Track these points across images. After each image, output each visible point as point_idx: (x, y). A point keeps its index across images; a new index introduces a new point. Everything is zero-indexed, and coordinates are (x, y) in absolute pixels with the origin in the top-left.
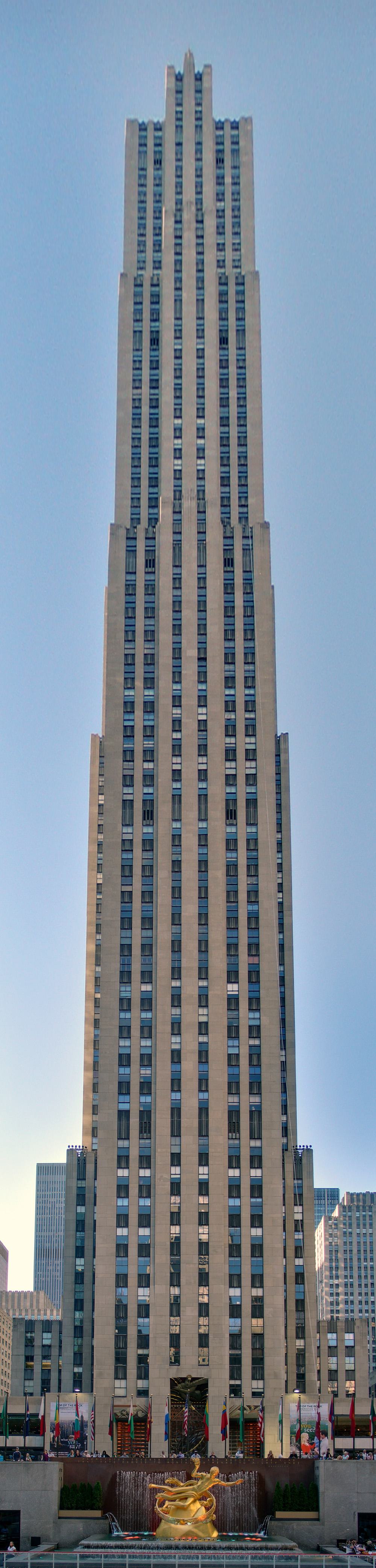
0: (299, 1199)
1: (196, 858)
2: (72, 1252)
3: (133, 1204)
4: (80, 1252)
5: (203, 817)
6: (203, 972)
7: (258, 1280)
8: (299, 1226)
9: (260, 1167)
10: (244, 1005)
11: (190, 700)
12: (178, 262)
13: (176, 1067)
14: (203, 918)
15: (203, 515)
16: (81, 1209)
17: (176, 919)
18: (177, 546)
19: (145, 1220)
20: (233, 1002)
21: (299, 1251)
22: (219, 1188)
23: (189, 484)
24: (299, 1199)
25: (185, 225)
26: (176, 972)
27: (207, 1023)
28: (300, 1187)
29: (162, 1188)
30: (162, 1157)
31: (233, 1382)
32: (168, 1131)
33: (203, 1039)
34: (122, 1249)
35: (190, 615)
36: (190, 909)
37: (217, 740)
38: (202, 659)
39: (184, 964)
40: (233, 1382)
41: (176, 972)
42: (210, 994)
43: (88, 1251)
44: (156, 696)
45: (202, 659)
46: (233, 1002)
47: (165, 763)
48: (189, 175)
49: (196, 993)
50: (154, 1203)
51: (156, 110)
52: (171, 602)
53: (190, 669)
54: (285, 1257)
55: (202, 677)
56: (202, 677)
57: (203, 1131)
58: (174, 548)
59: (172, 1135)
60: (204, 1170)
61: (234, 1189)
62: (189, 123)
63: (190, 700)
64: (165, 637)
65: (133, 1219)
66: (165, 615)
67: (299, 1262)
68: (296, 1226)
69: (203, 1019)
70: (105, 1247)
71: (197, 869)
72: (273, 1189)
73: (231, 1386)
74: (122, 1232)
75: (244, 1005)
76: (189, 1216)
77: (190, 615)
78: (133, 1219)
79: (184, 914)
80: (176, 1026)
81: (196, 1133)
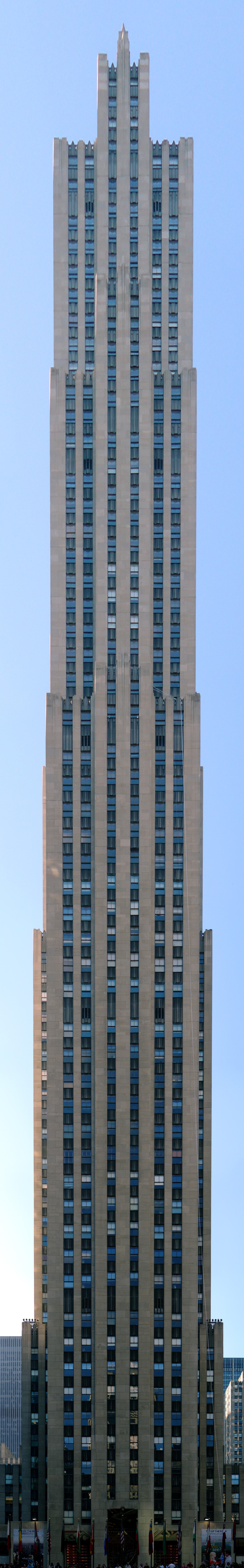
0: (211, 1365)
1: (128, 1056)
2: (28, 1408)
3: (77, 1368)
4: (34, 1408)
5: (134, 1016)
6: (134, 1165)
7: (177, 1431)
8: (210, 1387)
9: (180, 1337)
10: (168, 1195)
11: (123, 894)
12: (112, 355)
13: (111, 1251)
14: (134, 1113)
15: (136, 684)
16: (35, 1373)
17: (111, 1115)
18: (111, 720)
19: (87, 1381)
20: (159, 1192)
21: (210, 1408)
22: (147, 1355)
23: (123, 647)
24: (211, 1365)
25: (119, 302)
26: (111, 1165)
27: (137, 1212)
28: (212, 1355)
29: (101, 1355)
30: (100, 1329)
31: (157, 1513)
33: (134, 1226)
34: (68, 1405)
35: (123, 800)
36: (123, 1106)
37: (148, 937)
38: (135, 850)
39: (118, 1157)
40: (157, 1513)
41: (111, 1165)
42: (140, 1185)
43: (41, 1408)
44: (92, 889)
45: (135, 850)
46: (159, 1192)
47: (101, 961)
49: (128, 1184)
50: (94, 1367)
51: (86, 129)
52: (106, 785)
53: (123, 860)
54: (199, 1412)
55: (135, 869)
56: (135, 869)
57: (134, 1306)
58: (108, 723)
59: (109, 1310)
60: (134, 1340)
61: (159, 1355)
62: (123, 147)
63: (123, 894)
64: (100, 825)
65: (78, 1381)
66: (100, 799)
67: (210, 1416)
68: (208, 1387)
69: (134, 1208)
70: (54, 1404)
71: (129, 1067)
72: (191, 1356)
73: (155, 1515)
74: (69, 1391)
75: (168, 1195)
76: (122, 1378)
77: (123, 800)
78: (78, 1381)
79: (118, 1110)
80: (111, 1214)
81: (128, 1307)
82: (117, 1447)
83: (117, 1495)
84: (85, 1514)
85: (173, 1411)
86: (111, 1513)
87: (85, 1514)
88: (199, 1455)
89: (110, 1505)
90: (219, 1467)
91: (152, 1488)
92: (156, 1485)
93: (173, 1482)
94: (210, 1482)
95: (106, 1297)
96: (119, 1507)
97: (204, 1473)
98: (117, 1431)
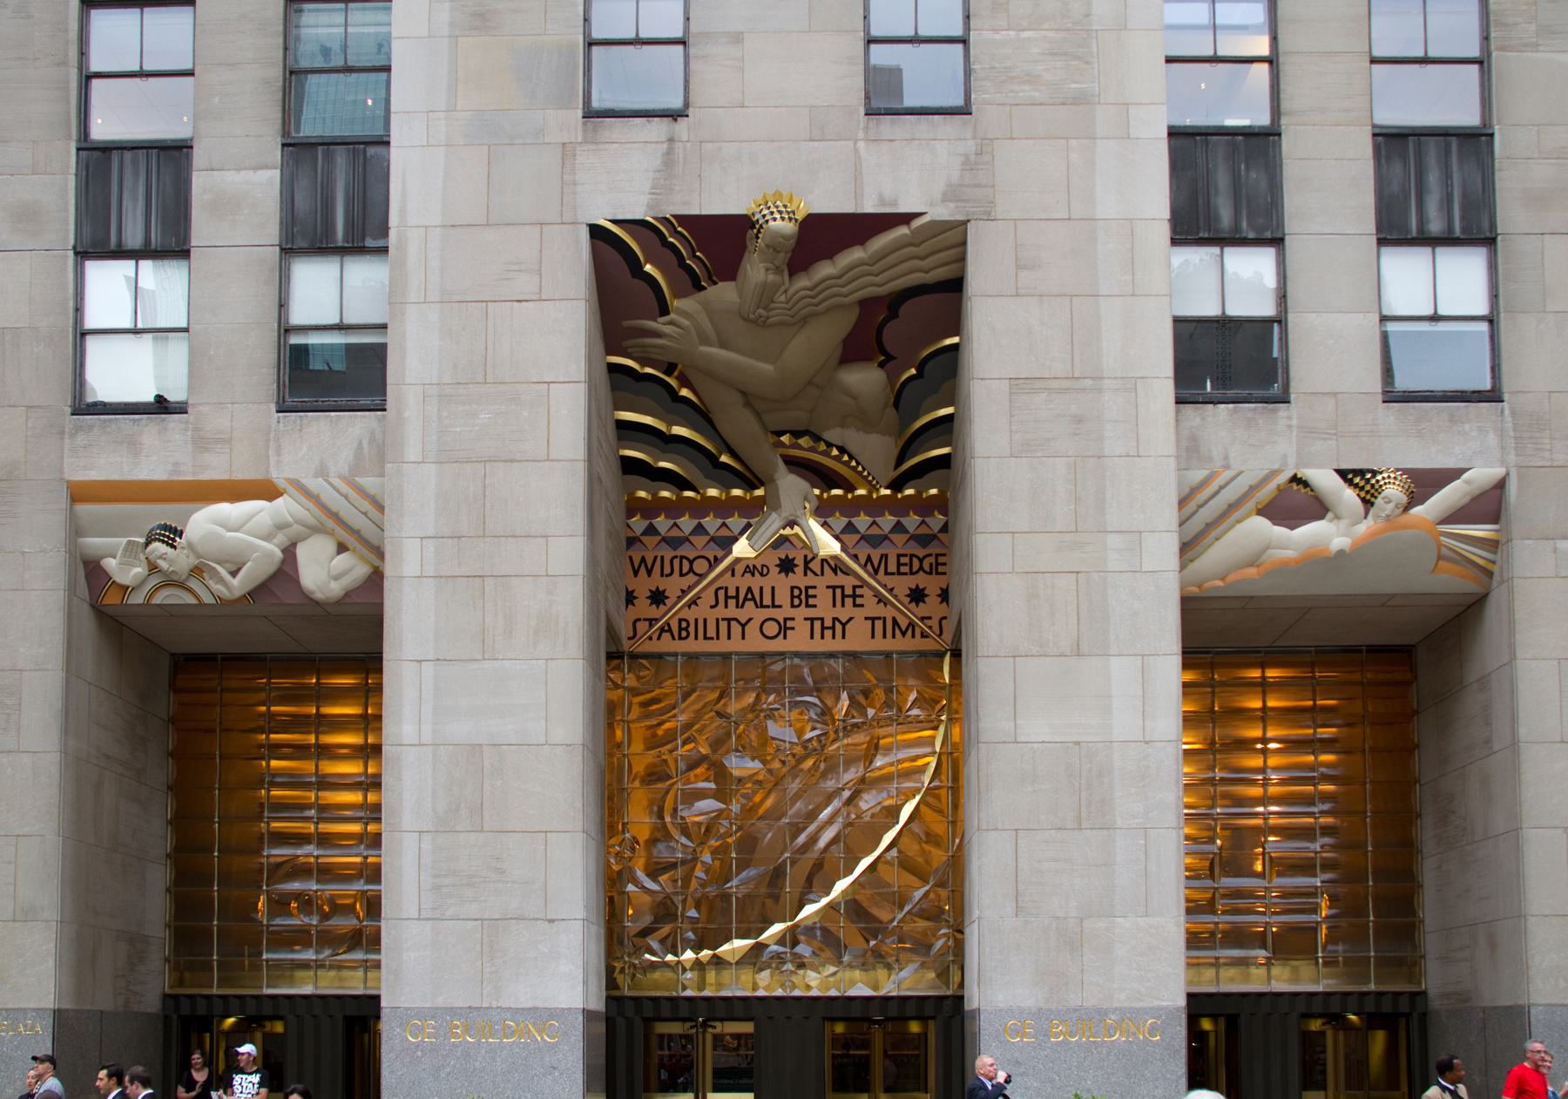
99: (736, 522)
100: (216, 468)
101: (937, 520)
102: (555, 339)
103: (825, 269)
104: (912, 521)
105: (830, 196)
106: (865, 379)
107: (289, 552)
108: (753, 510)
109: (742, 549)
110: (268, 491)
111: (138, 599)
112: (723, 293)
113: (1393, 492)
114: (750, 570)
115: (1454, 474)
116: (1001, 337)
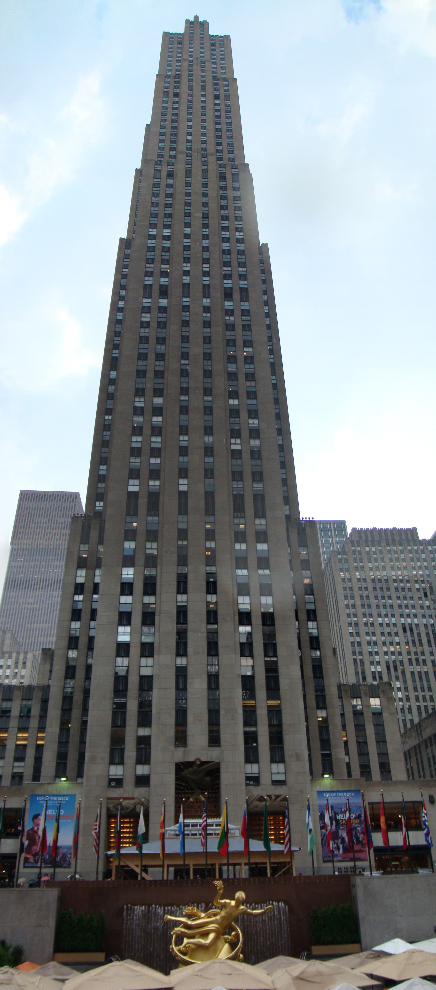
32: (175, 510)
48: (196, 85)
82: (190, 671)
83: (190, 741)
84: (142, 770)
85: (264, 624)
86: (180, 767)
87: (142, 770)
88: (303, 677)
89: (180, 755)
90: (332, 691)
91: (240, 729)
92: (246, 724)
93: (270, 719)
94: (321, 714)
95: (176, 501)
96: (192, 759)
97: (312, 701)
98: (190, 650)
99: (190, 796)
100: (126, 795)
101: (217, 795)
102: (171, 778)
103: (204, 767)
104: (214, 795)
105: (204, 759)
106: (208, 779)
107: (135, 807)
108: (192, 793)
109: (191, 800)
110: (133, 798)
111: (113, 813)
112: (191, 769)
113: (273, 798)
114: (192, 802)
115: (281, 795)
116: (225, 778)
